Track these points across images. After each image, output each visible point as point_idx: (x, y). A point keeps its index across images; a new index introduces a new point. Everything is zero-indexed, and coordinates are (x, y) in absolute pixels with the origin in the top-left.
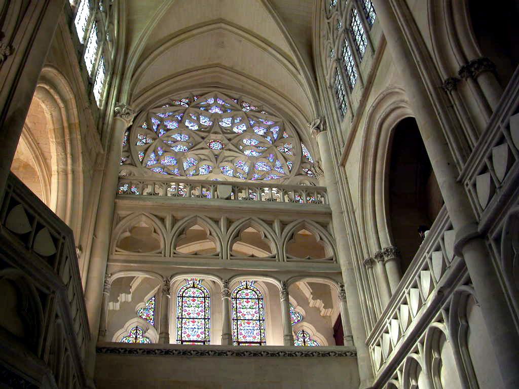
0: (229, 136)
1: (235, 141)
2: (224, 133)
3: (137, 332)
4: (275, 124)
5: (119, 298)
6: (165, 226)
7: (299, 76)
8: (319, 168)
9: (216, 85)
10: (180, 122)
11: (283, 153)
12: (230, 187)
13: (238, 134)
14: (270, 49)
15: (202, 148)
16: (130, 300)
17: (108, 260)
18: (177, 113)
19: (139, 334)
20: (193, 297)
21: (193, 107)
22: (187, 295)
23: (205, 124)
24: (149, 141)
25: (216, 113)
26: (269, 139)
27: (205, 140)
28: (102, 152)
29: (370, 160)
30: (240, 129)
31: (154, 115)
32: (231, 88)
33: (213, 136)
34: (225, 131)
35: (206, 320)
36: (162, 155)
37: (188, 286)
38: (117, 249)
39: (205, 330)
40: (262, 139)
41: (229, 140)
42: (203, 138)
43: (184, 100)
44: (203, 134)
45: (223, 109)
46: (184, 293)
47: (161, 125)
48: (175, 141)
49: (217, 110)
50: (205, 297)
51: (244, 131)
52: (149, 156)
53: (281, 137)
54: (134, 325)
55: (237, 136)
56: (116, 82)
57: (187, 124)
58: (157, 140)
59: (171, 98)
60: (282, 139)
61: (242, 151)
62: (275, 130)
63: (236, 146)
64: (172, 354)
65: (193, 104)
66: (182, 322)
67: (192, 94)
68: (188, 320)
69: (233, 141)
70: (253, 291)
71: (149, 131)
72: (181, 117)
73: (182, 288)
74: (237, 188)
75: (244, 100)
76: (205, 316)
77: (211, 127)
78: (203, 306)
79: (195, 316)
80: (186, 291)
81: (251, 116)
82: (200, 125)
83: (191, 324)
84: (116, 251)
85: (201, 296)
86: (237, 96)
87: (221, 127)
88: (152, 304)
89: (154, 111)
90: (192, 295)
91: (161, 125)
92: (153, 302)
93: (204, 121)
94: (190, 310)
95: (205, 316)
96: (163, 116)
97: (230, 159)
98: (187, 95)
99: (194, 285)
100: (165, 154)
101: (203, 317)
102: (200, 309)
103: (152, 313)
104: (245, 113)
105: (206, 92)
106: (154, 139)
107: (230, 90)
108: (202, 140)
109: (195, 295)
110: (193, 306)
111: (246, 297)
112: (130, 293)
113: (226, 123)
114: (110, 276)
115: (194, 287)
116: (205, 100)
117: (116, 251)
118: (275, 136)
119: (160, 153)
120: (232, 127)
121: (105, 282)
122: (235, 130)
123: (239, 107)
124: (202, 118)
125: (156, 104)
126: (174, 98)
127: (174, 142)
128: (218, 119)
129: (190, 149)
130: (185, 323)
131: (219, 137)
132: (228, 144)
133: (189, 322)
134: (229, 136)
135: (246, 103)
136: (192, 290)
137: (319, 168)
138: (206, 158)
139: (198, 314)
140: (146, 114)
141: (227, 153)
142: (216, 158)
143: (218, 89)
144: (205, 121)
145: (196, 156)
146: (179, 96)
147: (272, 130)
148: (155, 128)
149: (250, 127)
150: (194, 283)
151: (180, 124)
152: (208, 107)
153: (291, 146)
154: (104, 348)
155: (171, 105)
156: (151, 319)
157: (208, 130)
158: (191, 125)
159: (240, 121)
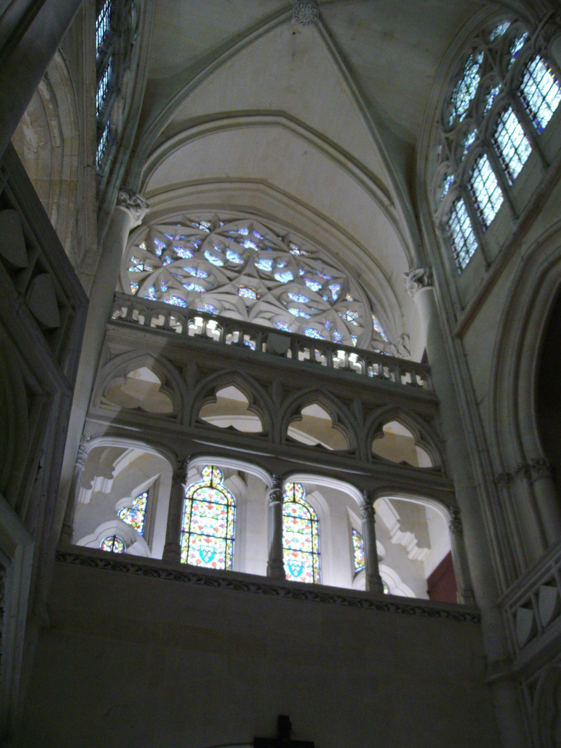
0: (270, 284)
1: (277, 292)
2: (261, 278)
3: (113, 544)
4: (335, 279)
5: (92, 483)
6: (185, 380)
7: (392, 209)
8: (404, 347)
9: (254, 212)
10: (197, 252)
11: (346, 322)
12: (288, 340)
13: (282, 285)
14: (350, 165)
15: (228, 293)
16: (108, 490)
17: (88, 414)
18: (193, 238)
19: (116, 548)
20: (210, 502)
21: (217, 234)
22: (200, 498)
23: (234, 261)
24: (148, 269)
25: (250, 249)
26: (325, 298)
27: (234, 282)
28: (95, 247)
29: (517, 325)
30: (285, 277)
31: (160, 235)
32: (275, 219)
33: (244, 279)
34: (263, 276)
35: (229, 542)
36: (167, 292)
37: (203, 484)
38: (104, 400)
39: (226, 557)
40: (317, 298)
41: (269, 289)
42: (230, 280)
43: (204, 223)
44: (231, 274)
45: (261, 245)
46: (195, 494)
47: (169, 248)
48: (188, 276)
50: (228, 506)
51: (290, 282)
52: (146, 289)
53: (342, 298)
54: (111, 533)
56: (125, 158)
57: (207, 255)
58: (161, 270)
59: (189, 216)
60: (344, 302)
61: (287, 308)
62: (335, 289)
63: (279, 299)
64: (186, 580)
65: (218, 230)
66: (189, 538)
67: (218, 217)
68: (200, 537)
69: (275, 294)
70: (304, 506)
71: (150, 255)
72: (200, 246)
73: (193, 486)
74: (299, 342)
75: (292, 239)
76: (227, 534)
77: (243, 267)
78: (225, 518)
79: (211, 532)
80: (199, 491)
82: (226, 261)
83: (204, 543)
84: (102, 403)
85: (221, 502)
86: (282, 233)
87: (258, 270)
88: (143, 503)
89: (162, 228)
90: (208, 499)
91: (169, 248)
92: (144, 500)
94: (202, 522)
95: (227, 534)
96: (171, 238)
97: (268, 315)
98: (210, 216)
99: (211, 484)
100: (172, 291)
101: (224, 536)
102: (220, 522)
103: (142, 518)
104: (294, 256)
105: (239, 217)
106: (156, 267)
108: (228, 281)
109: (212, 500)
110: (208, 515)
111: (293, 515)
112: (111, 477)
113: (265, 266)
114: (89, 438)
115: (211, 487)
116: (235, 228)
117: (102, 403)
118: (335, 297)
119: (164, 289)
120: (273, 272)
121: (79, 448)
122: (277, 277)
123: (284, 247)
124: (228, 253)
125: (164, 219)
126: (192, 217)
127: (185, 277)
128: (253, 258)
129: (208, 290)
130: (194, 542)
131: (254, 282)
132: (266, 294)
133: (200, 540)
134: (270, 284)
136: (209, 491)
137: (404, 347)
138: (232, 307)
139: (216, 530)
140: (148, 230)
141: (263, 306)
142: (248, 312)
143: (256, 218)
144: (233, 258)
145: (217, 302)
146: (198, 215)
148: (159, 253)
149: (298, 280)
150: (212, 481)
151: (197, 254)
152: (239, 240)
153: (356, 315)
154: (70, 555)
155: (183, 225)
156: (139, 527)
157: (239, 270)
159: (285, 266)
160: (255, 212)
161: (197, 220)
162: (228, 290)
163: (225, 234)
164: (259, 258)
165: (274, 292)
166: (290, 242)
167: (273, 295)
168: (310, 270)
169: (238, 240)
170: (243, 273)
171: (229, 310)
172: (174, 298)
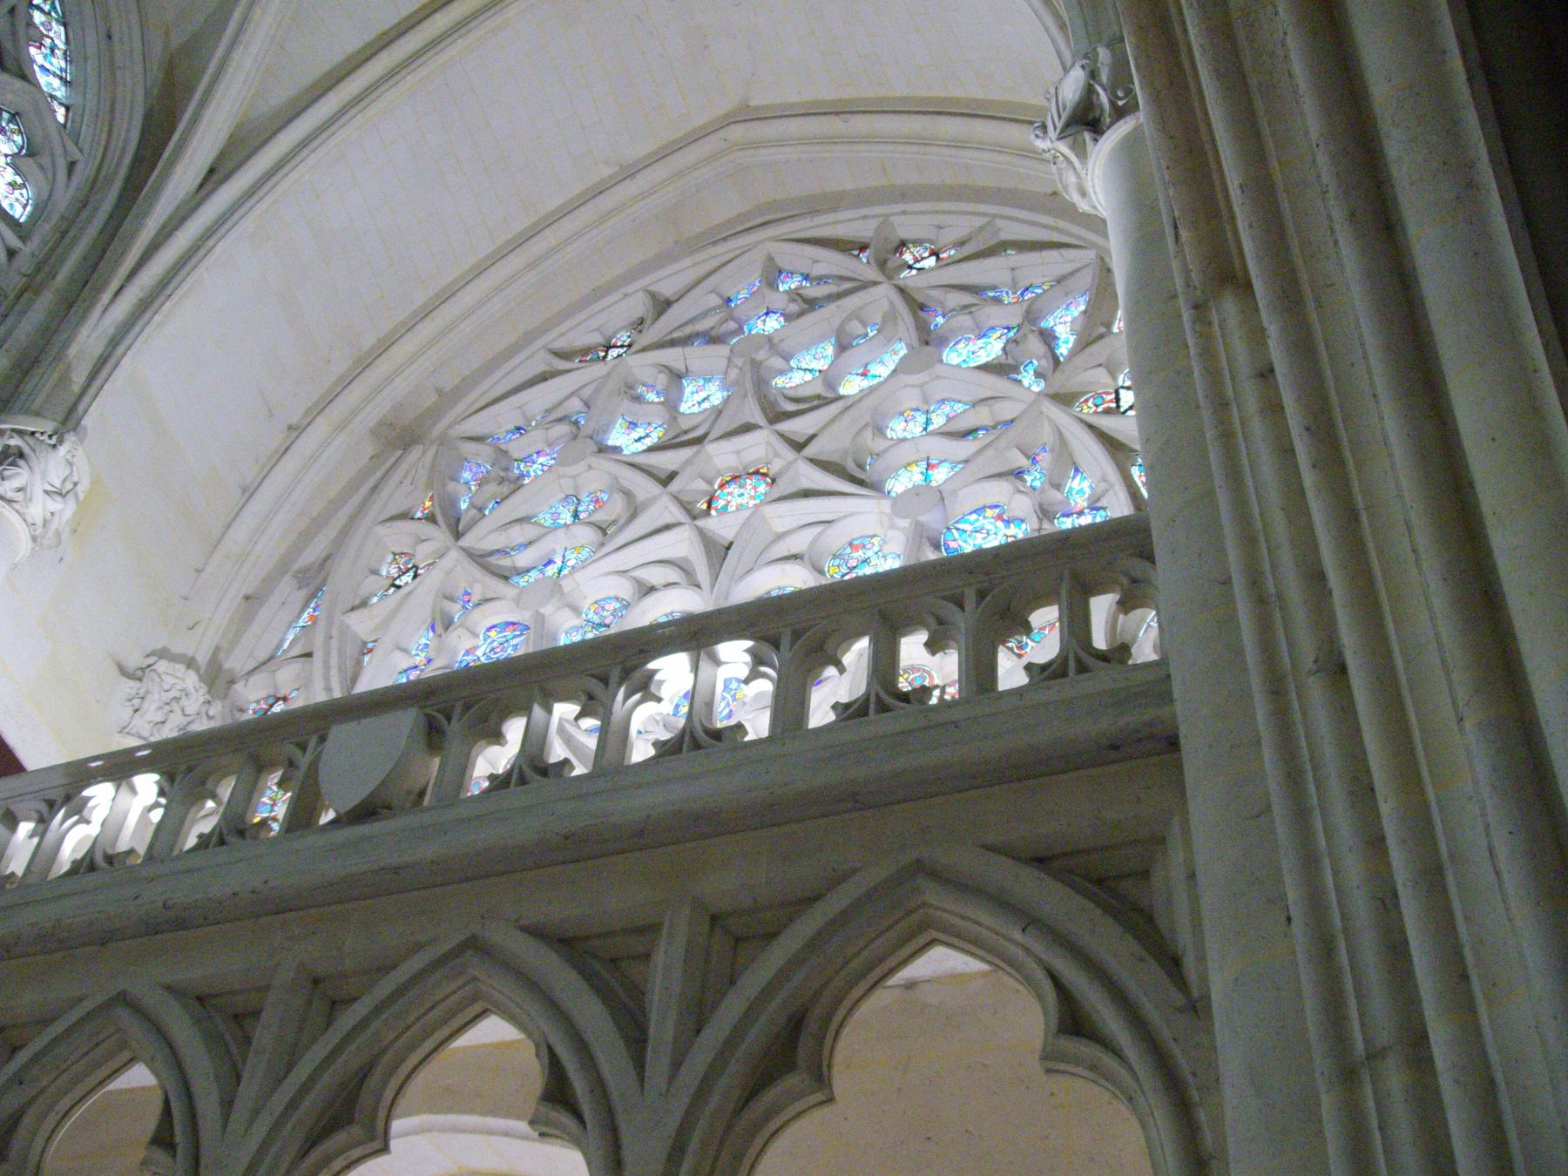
33: (723, 455)
49: (773, 324)
55: (847, 408)
59: (560, 344)
71: (427, 529)
75: (903, 234)
81: (935, 293)
93: (703, 395)
107: (834, 210)
108: (652, 488)
131: (759, 446)
135: (918, 242)
146: (594, 323)
147: (1048, 323)
158: (636, 434)
160: (768, 218)
161: (597, 338)
162: (669, 519)
163: (675, 335)
164: (787, 358)
165: (809, 451)
166: (903, 244)
167: (814, 462)
168: (967, 299)
169: (713, 333)
170: (712, 436)
171: (668, 585)
172: (493, 634)
